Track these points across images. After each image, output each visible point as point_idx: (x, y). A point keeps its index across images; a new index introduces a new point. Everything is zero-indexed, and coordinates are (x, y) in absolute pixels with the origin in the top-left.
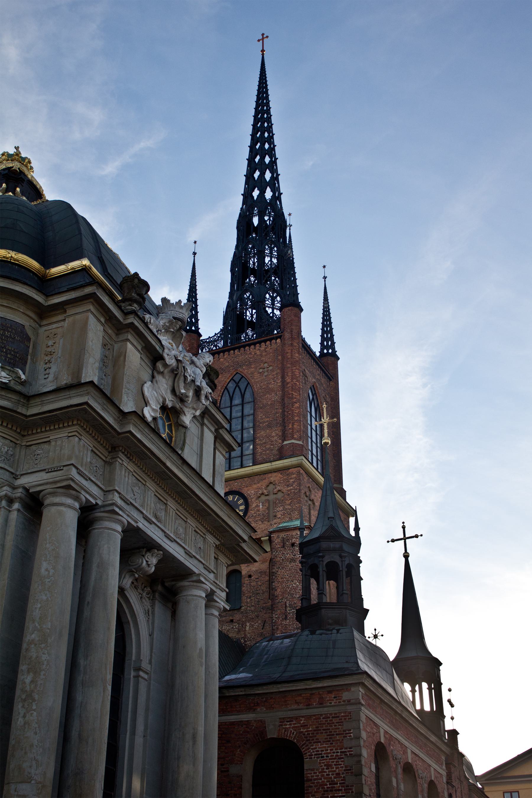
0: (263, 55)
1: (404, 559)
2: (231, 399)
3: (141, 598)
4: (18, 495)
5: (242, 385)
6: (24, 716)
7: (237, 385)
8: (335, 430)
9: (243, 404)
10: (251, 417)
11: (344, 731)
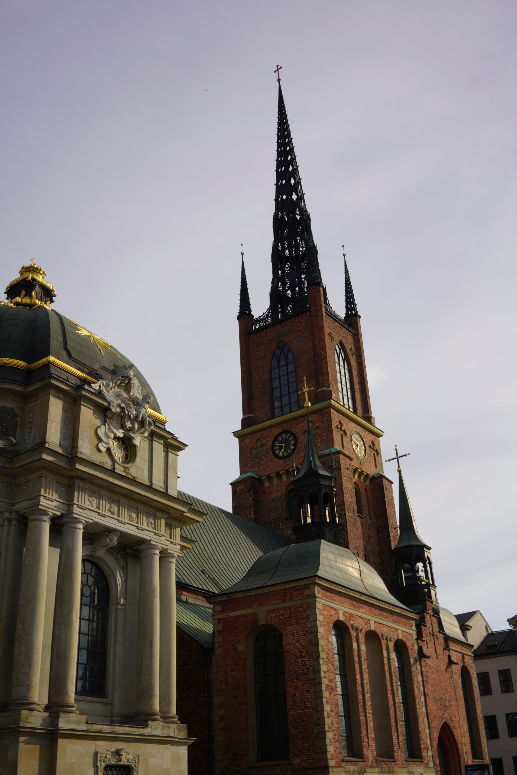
0: (279, 82)
1: (398, 473)
3: (117, 559)
4: (13, 516)
6: (18, 649)
7: (282, 351)
8: (361, 373)
9: (287, 365)
10: (294, 374)
11: (307, 616)
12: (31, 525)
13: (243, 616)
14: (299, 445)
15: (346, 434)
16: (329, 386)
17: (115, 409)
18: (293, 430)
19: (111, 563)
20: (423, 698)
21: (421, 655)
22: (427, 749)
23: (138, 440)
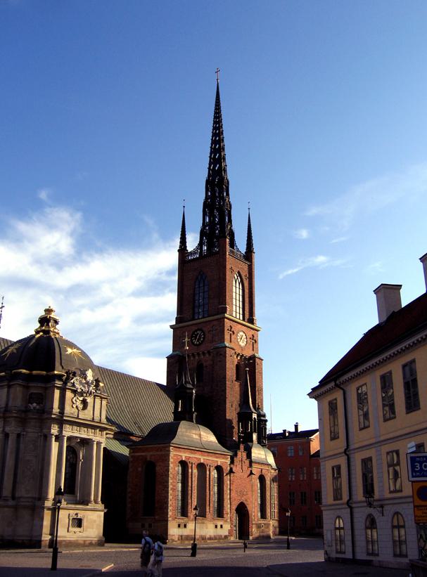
2: (199, 282)
5: (204, 277)
12: (48, 438)
13: (141, 456)
14: (206, 339)
15: (234, 333)
16: (225, 304)
17: (79, 390)
18: (204, 329)
19: (77, 447)
20: (229, 491)
21: (231, 471)
22: (227, 514)
23: (90, 400)
